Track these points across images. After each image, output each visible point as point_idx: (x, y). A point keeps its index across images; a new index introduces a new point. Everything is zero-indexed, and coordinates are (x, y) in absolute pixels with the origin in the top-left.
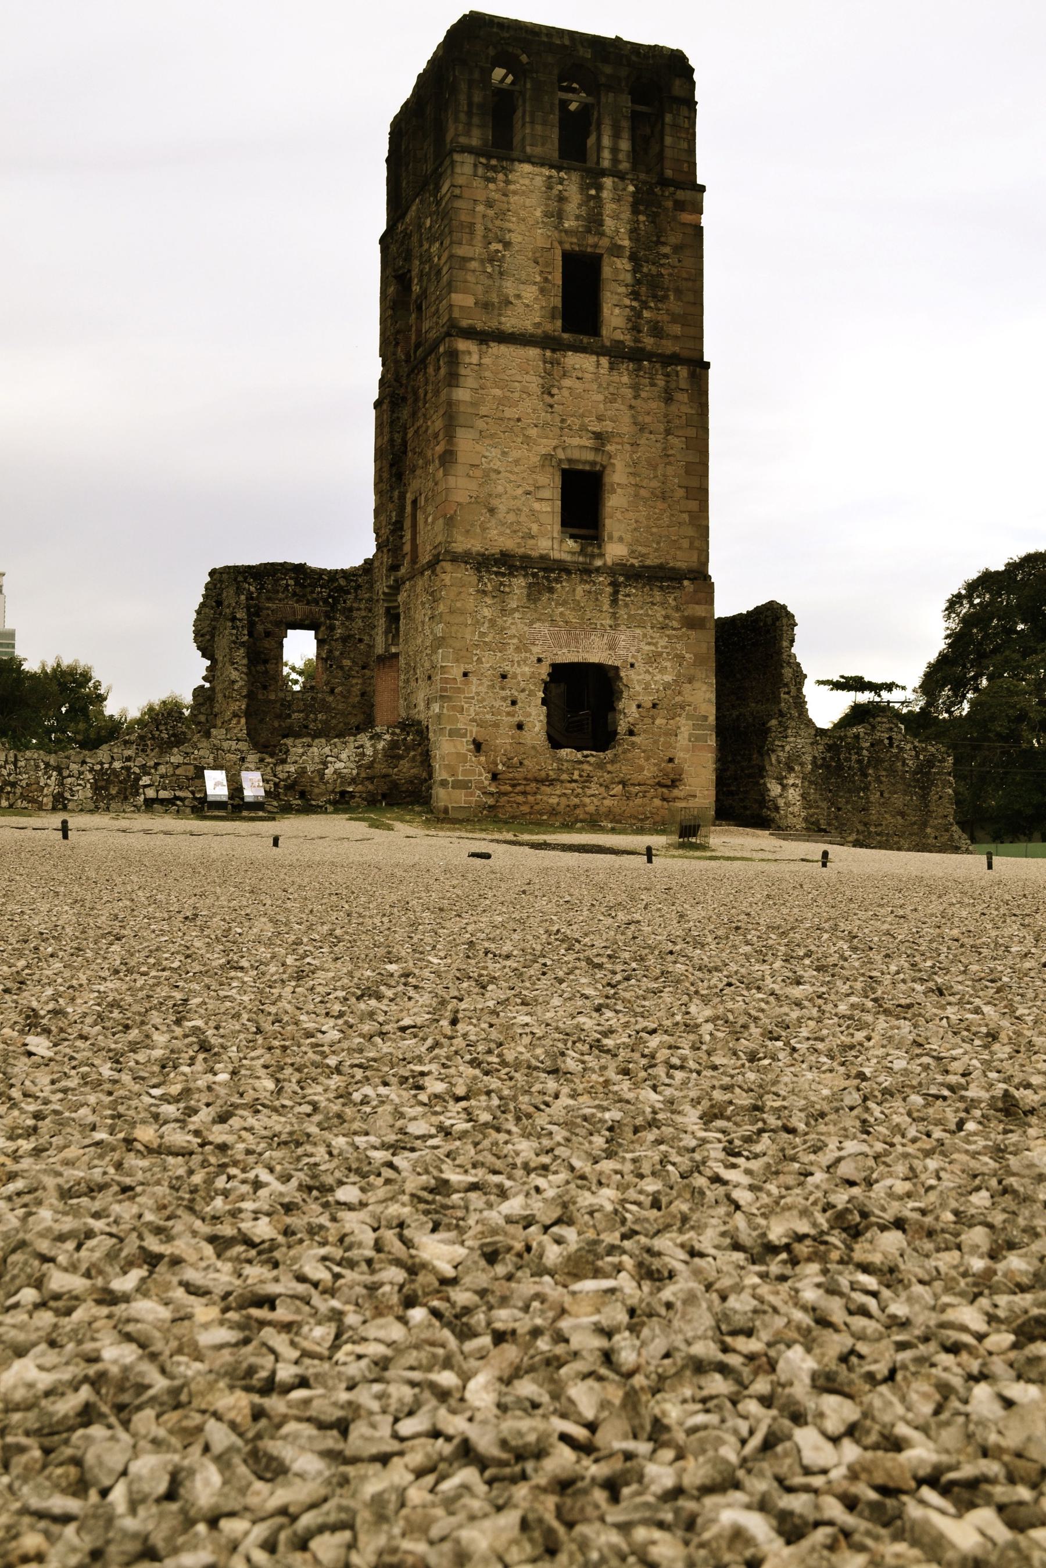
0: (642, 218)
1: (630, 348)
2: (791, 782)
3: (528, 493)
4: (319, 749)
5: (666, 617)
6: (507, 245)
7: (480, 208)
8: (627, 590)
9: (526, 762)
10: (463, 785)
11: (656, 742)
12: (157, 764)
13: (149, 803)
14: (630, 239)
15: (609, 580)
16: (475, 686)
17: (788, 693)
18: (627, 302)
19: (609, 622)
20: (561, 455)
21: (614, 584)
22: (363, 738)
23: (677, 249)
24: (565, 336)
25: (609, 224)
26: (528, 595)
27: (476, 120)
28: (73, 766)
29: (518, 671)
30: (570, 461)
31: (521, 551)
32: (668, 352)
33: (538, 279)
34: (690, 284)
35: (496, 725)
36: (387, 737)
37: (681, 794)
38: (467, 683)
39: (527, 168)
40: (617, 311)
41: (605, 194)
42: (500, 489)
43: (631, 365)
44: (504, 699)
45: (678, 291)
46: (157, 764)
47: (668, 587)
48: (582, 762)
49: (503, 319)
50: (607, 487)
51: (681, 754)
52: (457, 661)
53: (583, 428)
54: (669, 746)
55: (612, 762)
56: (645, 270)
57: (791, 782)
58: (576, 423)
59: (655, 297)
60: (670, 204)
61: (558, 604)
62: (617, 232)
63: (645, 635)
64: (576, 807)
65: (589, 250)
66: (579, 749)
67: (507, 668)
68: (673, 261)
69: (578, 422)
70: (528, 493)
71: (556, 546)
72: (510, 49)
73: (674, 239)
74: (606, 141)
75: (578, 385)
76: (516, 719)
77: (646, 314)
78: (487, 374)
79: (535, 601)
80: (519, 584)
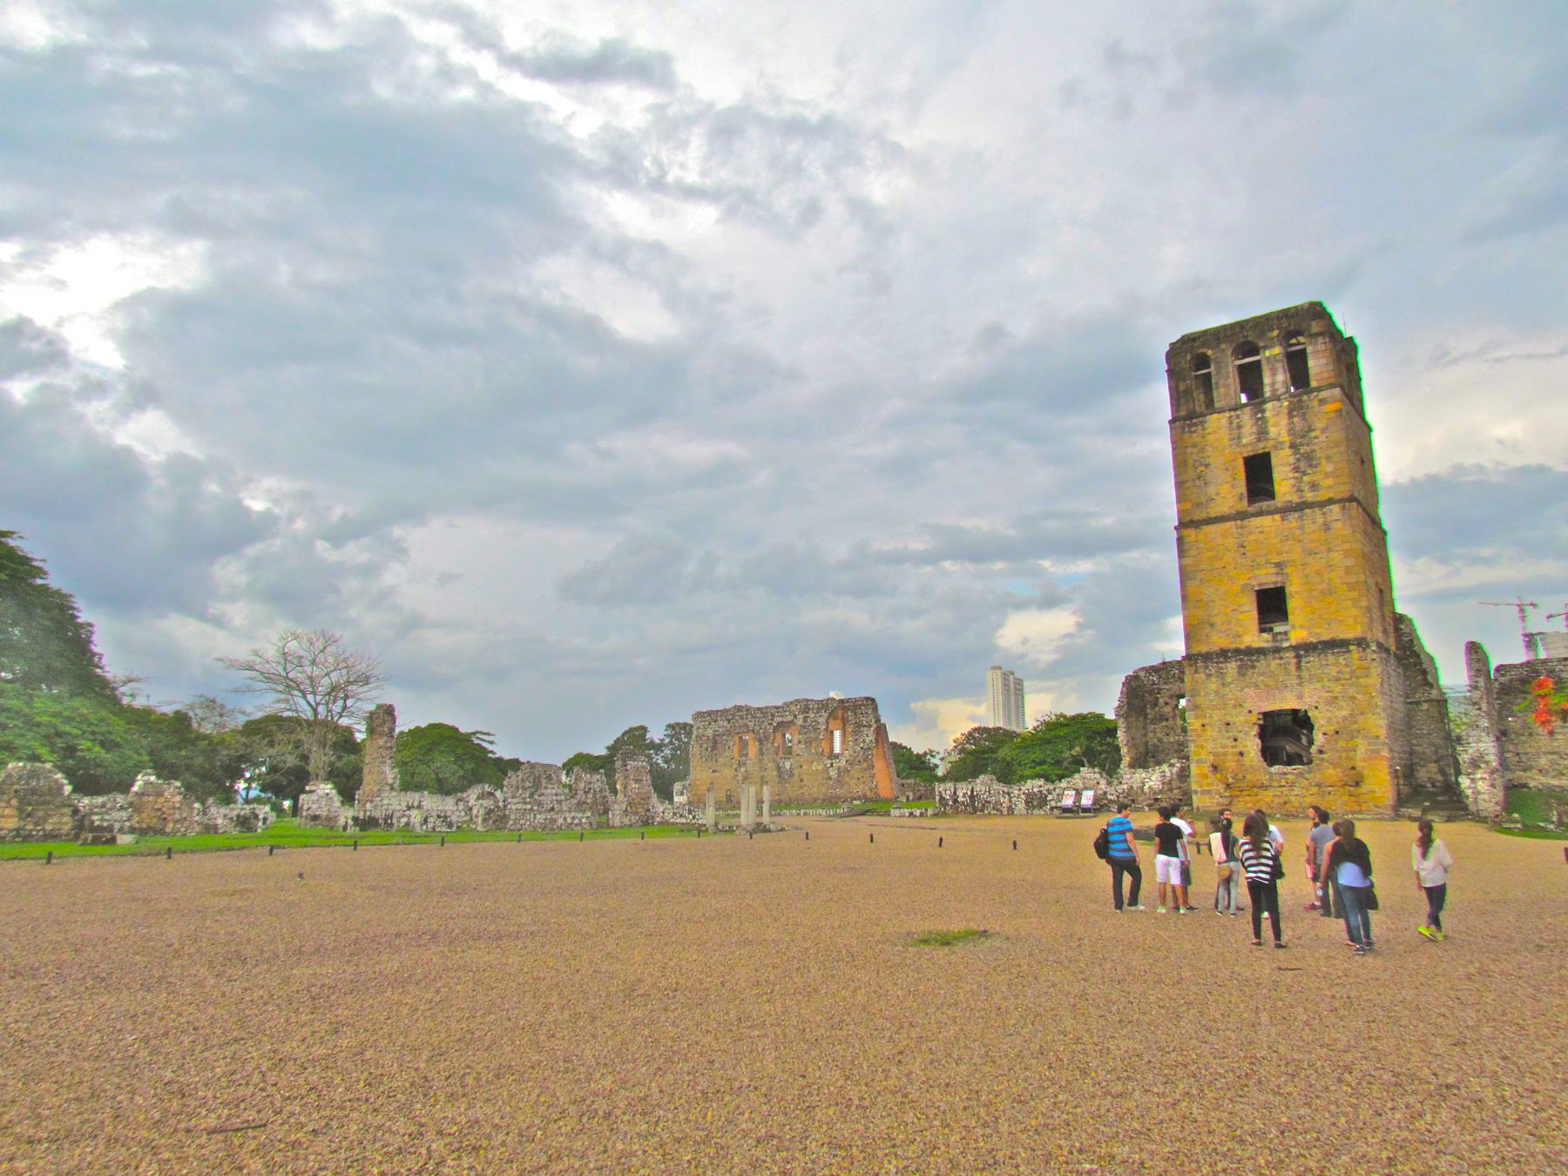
0: (1295, 419)
1: (1297, 504)
2: (1478, 776)
3: (1234, 610)
4: (1140, 774)
5: (1339, 672)
6: (1207, 466)
7: (1190, 450)
8: (1307, 659)
9: (1247, 776)
10: (1208, 792)
11: (1340, 757)
12: (1055, 789)
13: (1052, 809)
14: (1289, 435)
15: (1293, 654)
16: (1209, 732)
17: (1480, 709)
18: (1291, 475)
19: (1295, 681)
20: (1254, 582)
21: (1298, 657)
22: (1165, 767)
23: (1324, 430)
24: (1250, 509)
25: (1273, 431)
26: (1239, 673)
27: (1182, 401)
28: (1016, 792)
29: (1236, 720)
30: (1260, 585)
31: (1233, 646)
32: (1325, 498)
33: (1230, 479)
34: (1336, 450)
35: (1225, 754)
36: (1178, 765)
37: (1364, 791)
38: (1204, 731)
39: (1215, 416)
40: (1285, 482)
41: (1267, 414)
42: (1216, 611)
43: (1296, 515)
44: (1229, 738)
45: (1328, 458)
46: (1055, 789)
47: (1338, 652)
48: (1285, 774)
49: (1209, 510)
50: (1288, 596)
51: (1361, 764)
52: (1197, 717)
53: (1268, 562)
54: (1349, 758)
55: (1310, 772)
56: (1302, 451)
57: (1478, 776)
58: (1261, 560)
59: (1310, 466)
60: (1316, 403)
61: (1259, 675)
62: (1279, 434)
63: (1323, 687)
64: (1285, 803)
65: (1260, 452)
66: (1290, 765)
67: (1229, 719)
68: (1323, 438)
69: (1263, 559)
70: (1234, 610)
71: (1256, 639)
72: (1200, 351)
73: (1320, 425)
74: (1267, 380)
75: (1261, 537)
76: (1237, 750)
77: (1306, 479)
78: (1202, 545)
79: (1244, 675)
80: (1232, 667)
